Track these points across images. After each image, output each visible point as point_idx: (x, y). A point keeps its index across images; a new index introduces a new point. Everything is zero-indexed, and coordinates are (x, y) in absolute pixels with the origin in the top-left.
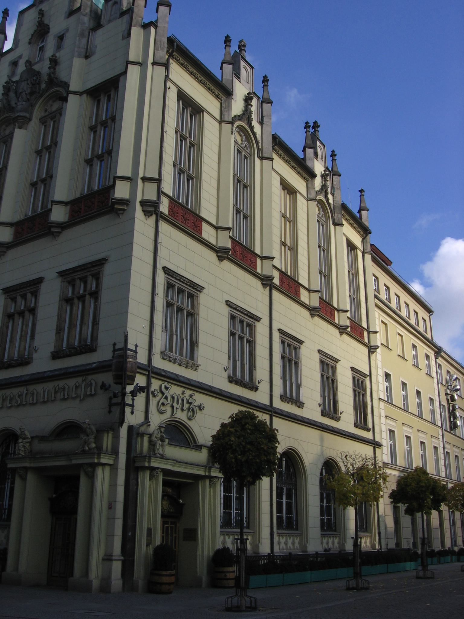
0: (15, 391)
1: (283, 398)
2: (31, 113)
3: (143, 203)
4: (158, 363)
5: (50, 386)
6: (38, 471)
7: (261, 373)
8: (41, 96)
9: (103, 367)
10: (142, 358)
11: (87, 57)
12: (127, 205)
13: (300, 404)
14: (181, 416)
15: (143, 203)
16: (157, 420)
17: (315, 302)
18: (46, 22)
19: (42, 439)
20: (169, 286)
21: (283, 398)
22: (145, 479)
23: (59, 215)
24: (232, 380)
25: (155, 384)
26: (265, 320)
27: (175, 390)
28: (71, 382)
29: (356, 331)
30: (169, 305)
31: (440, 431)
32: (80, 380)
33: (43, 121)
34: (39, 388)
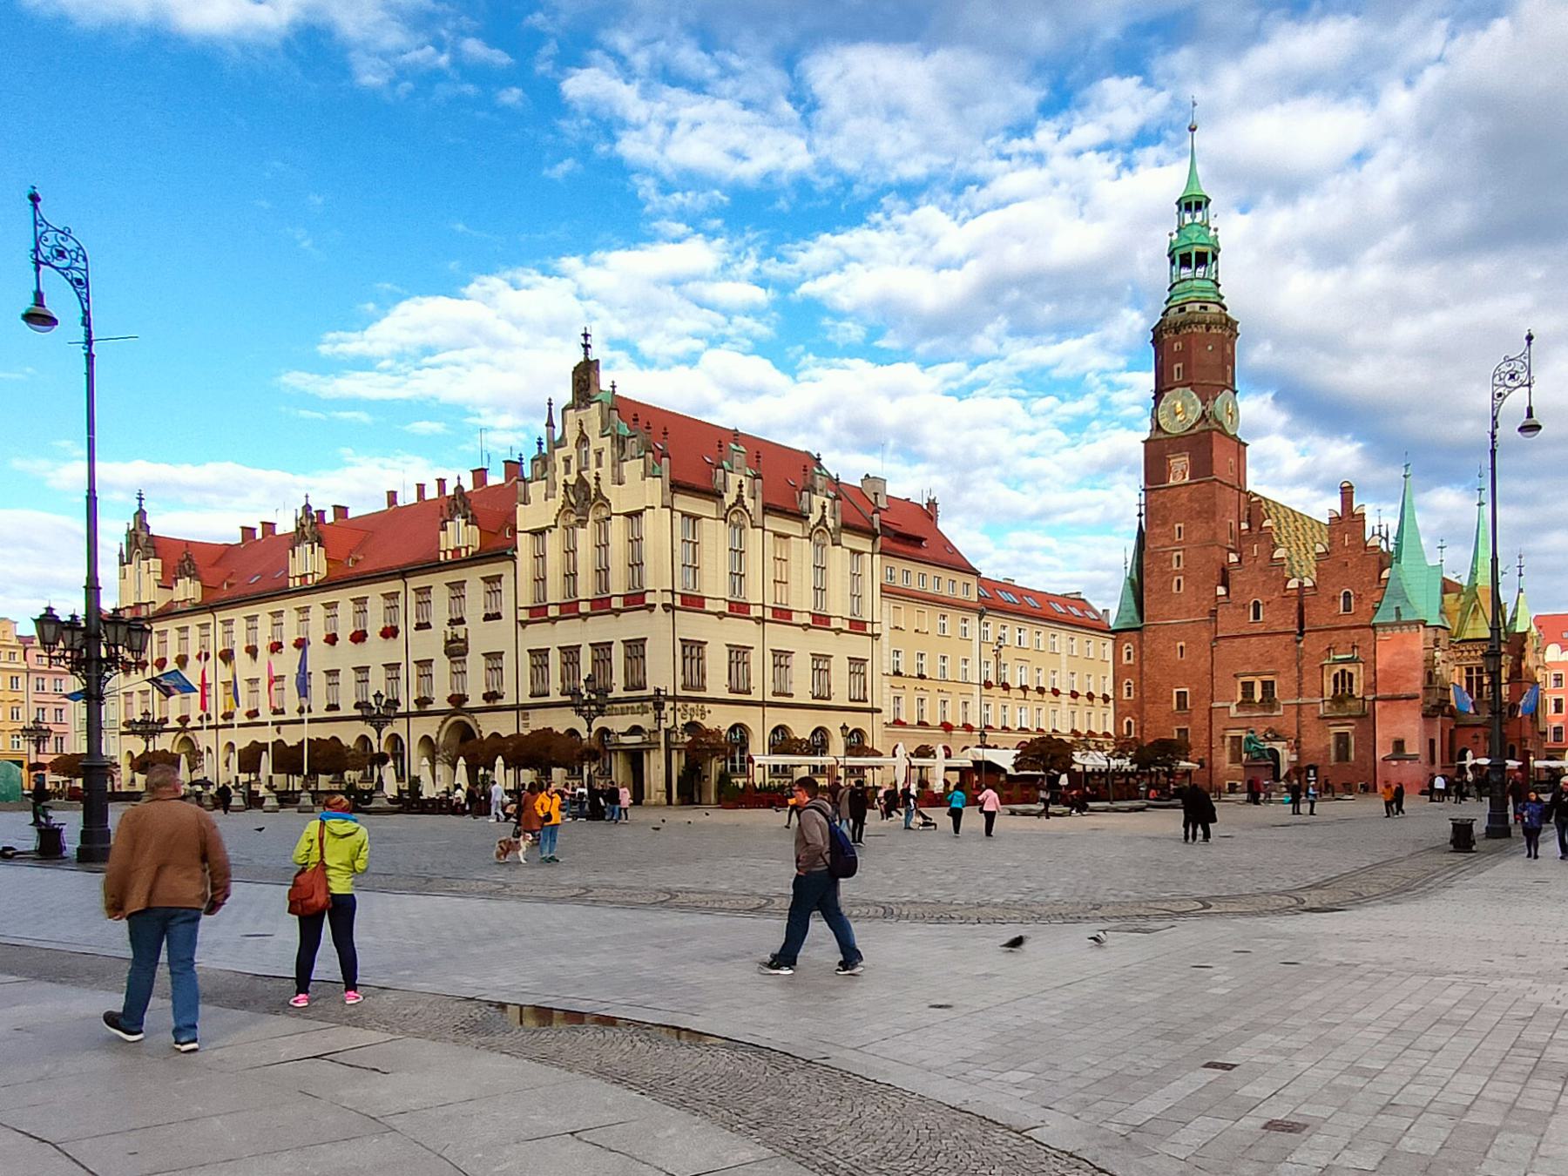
1: (774, 694)
4: (680, 693)
7: (755, 682)
9: (649, 699)
10: (671, 693)
14: (696, 718)
19: (624, 734)
20: (684, 647)
21: (774, 694)
22: (674, 753)
23: (617, 603)
24: (731, 691)
25: (679, 705)
26: (758, 646)
27: (691, 705)
28: (635, 705)
29: (858, 626)
30: (684, 658)
34: (618, 706)
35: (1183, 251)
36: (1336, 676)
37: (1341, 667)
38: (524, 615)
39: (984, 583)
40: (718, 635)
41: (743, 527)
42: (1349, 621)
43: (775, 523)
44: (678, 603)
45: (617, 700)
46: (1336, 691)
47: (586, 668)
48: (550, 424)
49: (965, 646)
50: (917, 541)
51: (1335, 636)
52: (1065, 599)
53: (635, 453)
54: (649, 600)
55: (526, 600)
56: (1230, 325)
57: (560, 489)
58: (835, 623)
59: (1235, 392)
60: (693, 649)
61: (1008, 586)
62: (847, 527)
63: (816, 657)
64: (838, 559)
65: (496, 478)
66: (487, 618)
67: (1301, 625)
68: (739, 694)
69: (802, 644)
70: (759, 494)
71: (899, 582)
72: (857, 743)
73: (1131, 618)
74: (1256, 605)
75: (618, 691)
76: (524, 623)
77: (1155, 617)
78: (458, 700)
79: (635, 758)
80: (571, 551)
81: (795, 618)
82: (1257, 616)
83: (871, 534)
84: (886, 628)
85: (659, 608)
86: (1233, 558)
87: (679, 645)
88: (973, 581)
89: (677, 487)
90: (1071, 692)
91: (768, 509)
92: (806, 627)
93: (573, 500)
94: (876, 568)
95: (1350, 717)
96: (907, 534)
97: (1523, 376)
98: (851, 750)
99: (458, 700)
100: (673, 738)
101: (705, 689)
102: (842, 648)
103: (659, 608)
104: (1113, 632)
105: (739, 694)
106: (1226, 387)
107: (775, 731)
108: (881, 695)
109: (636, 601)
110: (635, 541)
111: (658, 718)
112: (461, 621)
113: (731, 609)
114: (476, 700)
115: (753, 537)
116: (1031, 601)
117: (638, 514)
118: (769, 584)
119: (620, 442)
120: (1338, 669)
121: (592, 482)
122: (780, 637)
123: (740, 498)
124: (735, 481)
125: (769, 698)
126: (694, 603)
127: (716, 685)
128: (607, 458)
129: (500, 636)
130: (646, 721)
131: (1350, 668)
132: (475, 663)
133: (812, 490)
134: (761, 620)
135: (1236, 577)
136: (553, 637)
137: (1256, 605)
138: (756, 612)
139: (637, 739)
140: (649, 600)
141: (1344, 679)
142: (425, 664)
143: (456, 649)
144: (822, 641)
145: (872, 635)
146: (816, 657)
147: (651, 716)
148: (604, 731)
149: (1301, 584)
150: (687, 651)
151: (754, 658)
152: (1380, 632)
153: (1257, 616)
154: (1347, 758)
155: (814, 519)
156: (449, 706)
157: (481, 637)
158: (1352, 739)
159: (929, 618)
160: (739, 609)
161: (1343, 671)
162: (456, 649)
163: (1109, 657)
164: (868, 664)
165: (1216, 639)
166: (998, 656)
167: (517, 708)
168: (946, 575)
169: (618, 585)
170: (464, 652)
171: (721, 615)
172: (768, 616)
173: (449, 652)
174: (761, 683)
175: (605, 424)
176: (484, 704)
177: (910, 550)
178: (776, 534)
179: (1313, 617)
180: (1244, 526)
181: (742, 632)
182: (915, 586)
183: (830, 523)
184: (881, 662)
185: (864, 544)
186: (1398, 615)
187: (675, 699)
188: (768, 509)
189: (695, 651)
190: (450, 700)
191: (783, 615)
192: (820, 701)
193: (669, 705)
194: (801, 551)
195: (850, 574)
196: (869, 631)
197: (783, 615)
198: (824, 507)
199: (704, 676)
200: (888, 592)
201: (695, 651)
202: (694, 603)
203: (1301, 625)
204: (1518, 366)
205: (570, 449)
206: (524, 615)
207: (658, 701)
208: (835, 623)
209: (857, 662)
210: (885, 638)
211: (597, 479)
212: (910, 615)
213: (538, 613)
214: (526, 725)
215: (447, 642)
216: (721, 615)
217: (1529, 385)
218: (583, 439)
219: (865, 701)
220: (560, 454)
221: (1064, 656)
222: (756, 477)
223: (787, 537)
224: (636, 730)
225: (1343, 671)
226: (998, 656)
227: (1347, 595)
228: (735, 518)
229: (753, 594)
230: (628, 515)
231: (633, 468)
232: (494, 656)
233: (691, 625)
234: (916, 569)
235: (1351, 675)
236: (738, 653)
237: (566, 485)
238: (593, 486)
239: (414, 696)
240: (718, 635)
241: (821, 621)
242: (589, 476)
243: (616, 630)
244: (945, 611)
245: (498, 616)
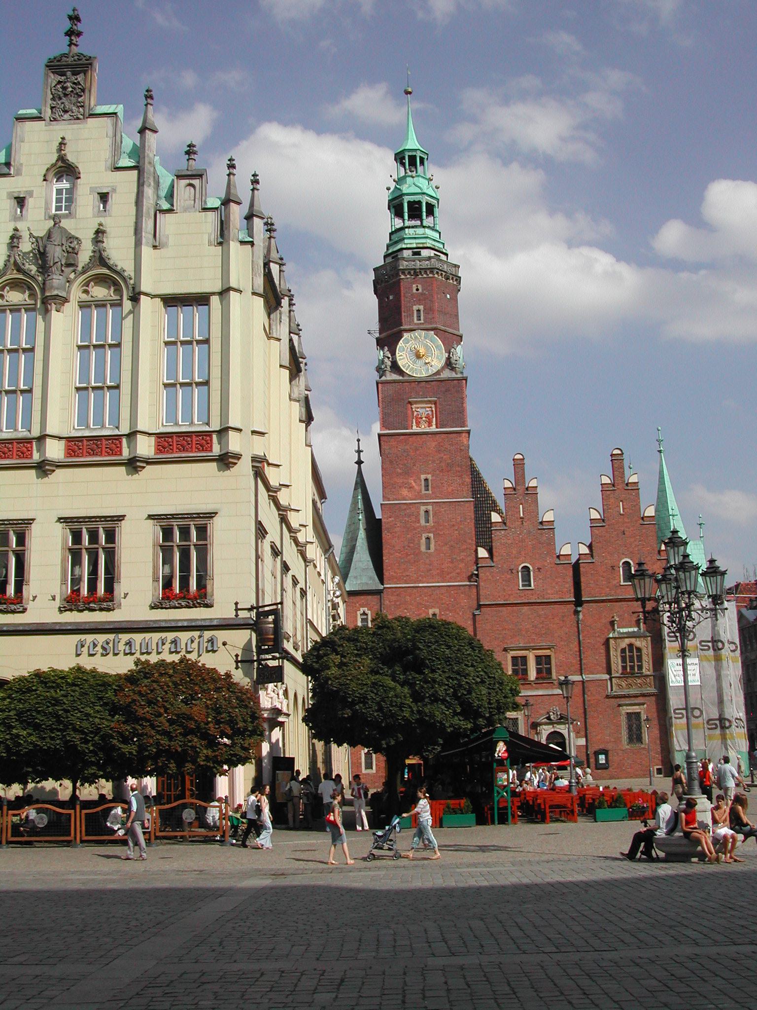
0: (101, 638)
2: (69, 292)
5: (156, 636)
8: (84, 272)
11: (155, 247)
12: (239, 459)
18: (71, 158)
32: (196, 634)
33: (83, 305)
46: (624, 668)
77: (399, 580)
120: (625, 643)
131: (638, 643)
135: (499, 539)
154: (640, 739)
161: (631, 646)
165: (479, 607)
225: (631, 646)
235: (639, 650)
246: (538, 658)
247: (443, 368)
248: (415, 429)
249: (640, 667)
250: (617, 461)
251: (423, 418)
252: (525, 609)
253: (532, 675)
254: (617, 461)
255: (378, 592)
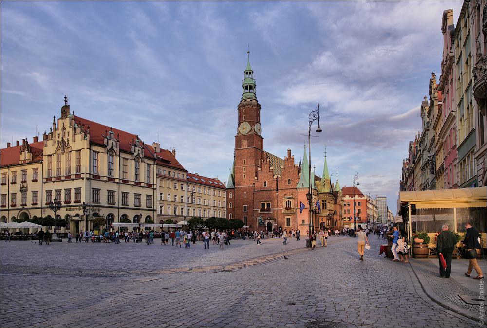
1: (122, 205)
3: (87, 178)
4: (92, 204)
6: (74, 221)
7: (116, 201)
9: (81, 206)
10: (88, 204)
13: (128, 205)
15: (87, 178)
16: (92, 213)
17: (133, 183)
20: (93, 191)
21: (122, 205)
22: (89, 222)
24: (108, 204)
25: (91, 208)
26: (117, 191)
27: (95, 208)
28: (78, 207)
29: (149, 186)
31: (186, 204)
35: (246, 85)
36: (287, 202)
37: (288, 200)
38: (44, 180)
39: (189, 174)
40: (105, 188)
41: (113, 156)
42: (290, 187)
43: (123, 155)
44: (91, 177)
45: (72, 206)
47: (53, 197)
48: (54, 123)
49: (182, 193)
50: (168, 162)
51: (286, 191)
52: (213, 180)
53: (79, 133)
54: (82, 176)
55: (45, 175)
56: (259, 105)
57: (57, 143)
58: (142, 185)
59: (260, 124)
60: (96, 191)
61: (196, 176)
62: (146, 157)
63: (136, 194)
64: (143, 166)
65: (41, 139)
66: (33, 181)
67: (277, 188)
68: (111, 205)
69: (131, 191)
70: (118, 146)
71: (162, 173)
72: (149, 220)
73: (231, 186)
74: (265, 182)
75: (72, 204)
76: (45, 183)
78: (24, 205)
79: (77, 223)
80: (59, 161)
81: (130, 183)
82: (265, 185)
83: (154, 159)
84: (158, 186)
85: (85, 179)
86: (259, 169)
87: (91, 190)
88: (185, 174)
89: (92, 143)
90: (213, 205)
91: (121, 151)
92: (133, 186)
93: (61, 146)
94: (154, 169)
95: (290, 213)
96: (166, 161)
97: (317, 116)
98: (146, 222)
99: (24, 205)
100: (89, 217)
101: (100, 203)
102: (144, 192)
103: (85, 179)
104: (227, 189)
105: (111, 205)
106: (257, 122)
107: (123, 216)
108: (157, 206)
109: (78, 176)
110: (79, 159)
111: (84, 211)
112: (25, 182)
113: (109, 179)
114: (29, 206)
115: (116, 159)
116: (203, 180)
117: (79, 151)
118: (121, 173)
119: (75, 129)
120: (287, 200)
121: (66, 141)
122: (125, 188)
123: (112, 148)
124: (111, 142)
125: (121, 206)
126: (97, 177)
127: (104, 201)
128: (71, 134)
129: (37, 186)
130: (81, 212)
131: (290, 200)
132: (29, 195)
133: (135, 146)
134: (118, 183)
135: (260, 174)
136: (53, 187)
137: (265, 182)
138: (117, 181)
139: (77, 218)
140: (82, 176)
141: (289, 203)
142: (14, 195)
143: (24, 190)
144: (138, 190)
145: (154, 189)
146: (136, 194)
147: (82, 211)
148: (68, 215)
149: (277, 177)
150: (94, 192)
151: (116, 194)
152: (298, 190)
153: (265, 185)
155: (136, 154)
156: (21, 207)
157: (32, 187)
158: (291, 219)
159: (172, 184)
160: (111, 180)
161: (288, 201)
162: (24, 190)
163: (225, 196)
164: (153, 197)
166: (192, 195)
167: (42, 208)
168: (177, 172)
169: (73, 172)
170: (26, 191)
171: (105, 181)
172: (121, 182)
173: (21, 191)
174: (117, 200)
175: (70, 124)
176: (31, 207)
177: (166, 164)
178: (124, 158)
179: (281, 186)
180: (262, 160)
181: (113, 187)
182: (167, 174)
183: (141, 156)
184: (157, 196)
185: (151, 162)
186: (303, 185)
187: (90, 206)
188: (121, 151)
189: (97, 192)
190: (21, 205)
191: (125, 182)
192: (137, 207)
193: (87, 208)
194: (131, 164)
195: (146, 171)
196: (153, 187)
197: (125, 182)
198: (139, 151)
199: (100, 199)
200: (158, 176)
201: (97, 192)
202: (97, 177)
203: (277, 188)
204: (316, 114)
205: (60, 131)
206: (44, 180)
207: (84, 206)
208: (142, 185)
209: (149, 197)
210: (158, 188)
211: (68, 140)
212: (165, 183)
213: (49, 180)
214: (45, 213)
215: (21, 188)
216: (105, 181)
217: (319, 119)
218: (64, 128)
219: (5, 206)
220: (57, 132)
221: (212, 195)
222: (118, 141)
223: (127, 159)
224: (77, 215)
225: (288, 201)
226: (192, 195)
227: (289, 180)
228: (111, 153)
229: (116, 175)
230: (77, 151)
231: (79, 137)
232: (35, 193)
233: (96, 184)
234: (167, 170)
236: (111, 193)
237: (58, 141)
238: (67, 142)
239: (10, 204)
240: (105, 188)
241: (137, 184)
242: (65, 139)
243: (72, 185)
244: (176, 182)
245: (37, 180)
246: (267, 204)
247: (250, 132)
248: (243, 148)
249: (290, 206)
250: (289, 152)
251: (245, 143)
252: (265, 192)
253: (266, 208)
254: (289, 152)
255: (234, 188)
